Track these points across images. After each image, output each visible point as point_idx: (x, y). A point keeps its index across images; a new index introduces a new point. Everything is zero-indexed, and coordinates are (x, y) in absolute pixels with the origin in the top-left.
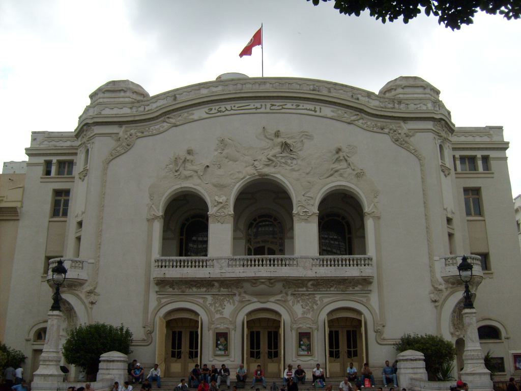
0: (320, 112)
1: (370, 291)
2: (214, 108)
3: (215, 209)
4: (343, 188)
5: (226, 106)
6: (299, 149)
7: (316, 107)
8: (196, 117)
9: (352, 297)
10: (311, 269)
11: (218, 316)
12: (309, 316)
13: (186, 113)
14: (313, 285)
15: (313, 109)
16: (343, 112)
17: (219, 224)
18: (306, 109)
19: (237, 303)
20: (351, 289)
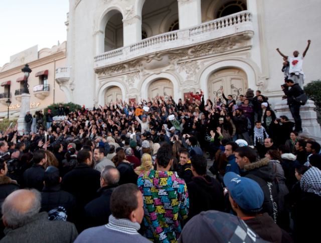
1: (251, 46)
3: (127, 15)
9: (230, 57)
10: (189, 39)
11: (130, 88)
12: (192, 79)
14: (192, 52)
17: (129, 25)
19: (141, 77)
20: (229, 49)
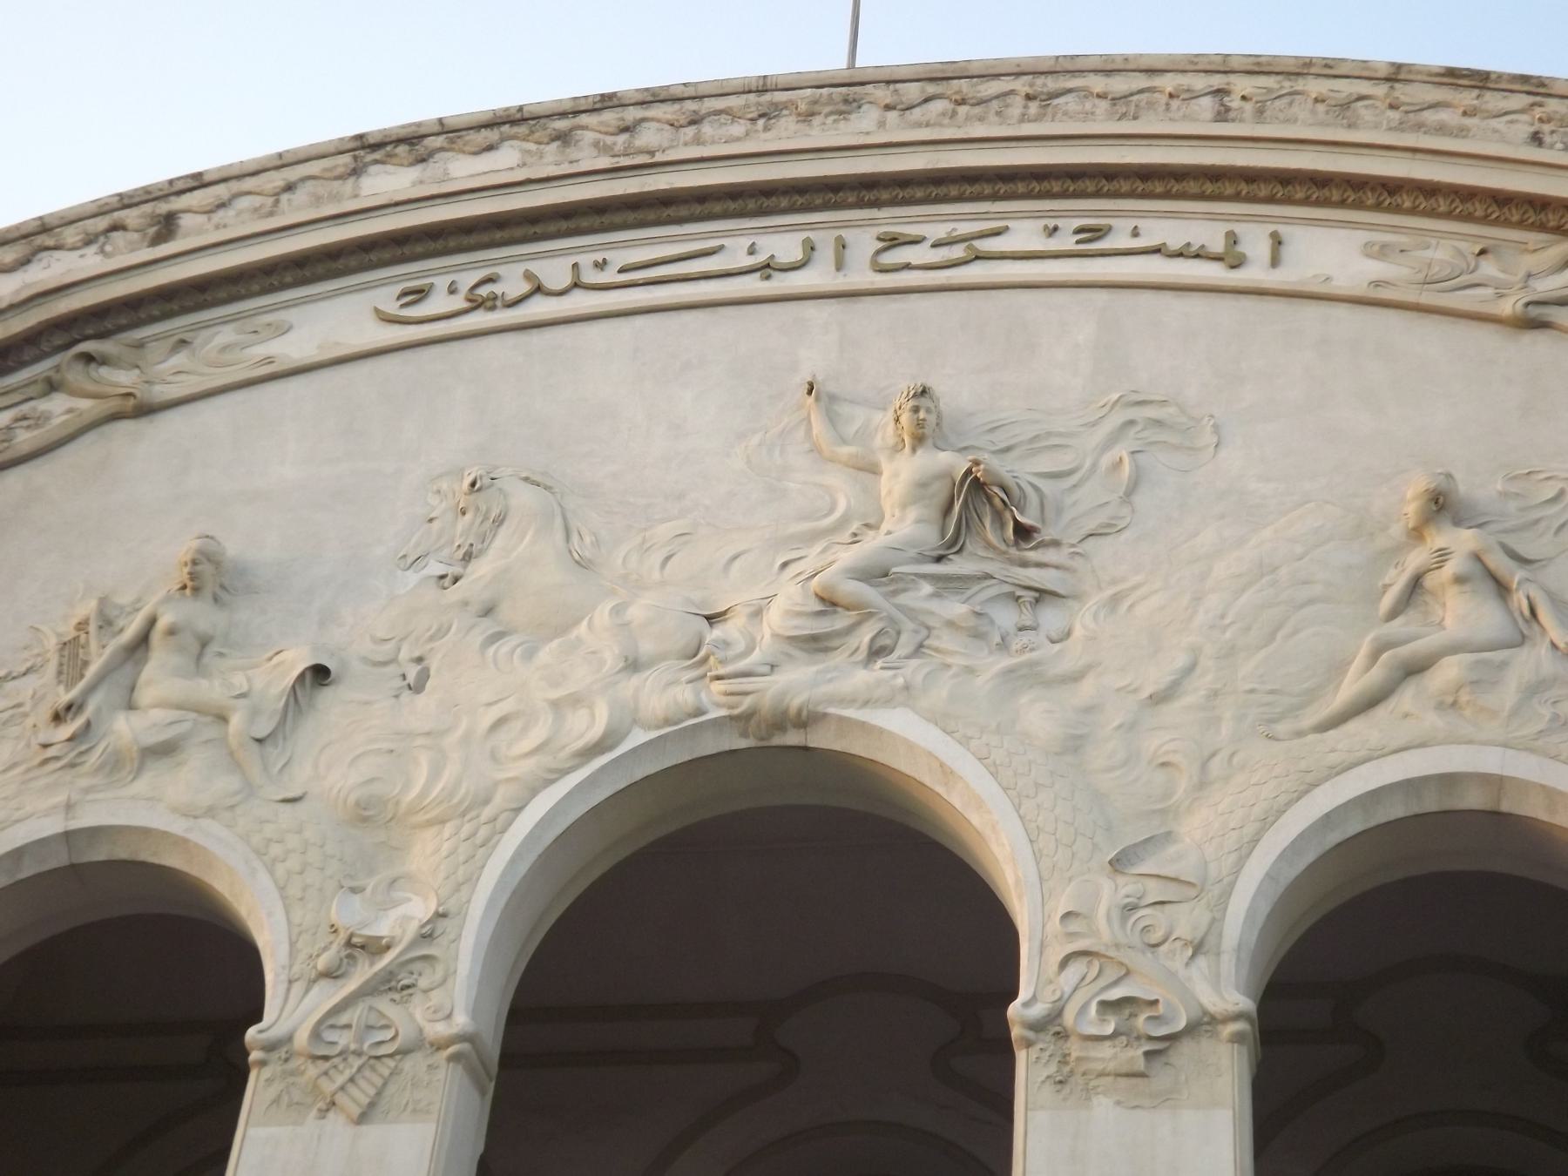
0: (1275, 261)
2: (442, 282)
4: (1473, 800)
5: (535, 267)
6: (1090, 525)
7: (1239, 228)
8: (294, 347)
13: (228, 328)
15: (1218, 246)
16: (1463, 245)
18: (1157, 250)
